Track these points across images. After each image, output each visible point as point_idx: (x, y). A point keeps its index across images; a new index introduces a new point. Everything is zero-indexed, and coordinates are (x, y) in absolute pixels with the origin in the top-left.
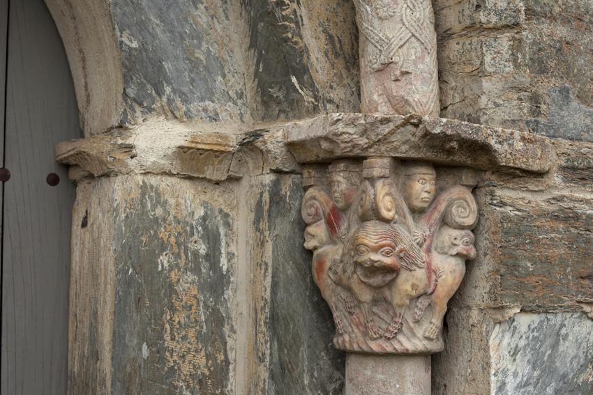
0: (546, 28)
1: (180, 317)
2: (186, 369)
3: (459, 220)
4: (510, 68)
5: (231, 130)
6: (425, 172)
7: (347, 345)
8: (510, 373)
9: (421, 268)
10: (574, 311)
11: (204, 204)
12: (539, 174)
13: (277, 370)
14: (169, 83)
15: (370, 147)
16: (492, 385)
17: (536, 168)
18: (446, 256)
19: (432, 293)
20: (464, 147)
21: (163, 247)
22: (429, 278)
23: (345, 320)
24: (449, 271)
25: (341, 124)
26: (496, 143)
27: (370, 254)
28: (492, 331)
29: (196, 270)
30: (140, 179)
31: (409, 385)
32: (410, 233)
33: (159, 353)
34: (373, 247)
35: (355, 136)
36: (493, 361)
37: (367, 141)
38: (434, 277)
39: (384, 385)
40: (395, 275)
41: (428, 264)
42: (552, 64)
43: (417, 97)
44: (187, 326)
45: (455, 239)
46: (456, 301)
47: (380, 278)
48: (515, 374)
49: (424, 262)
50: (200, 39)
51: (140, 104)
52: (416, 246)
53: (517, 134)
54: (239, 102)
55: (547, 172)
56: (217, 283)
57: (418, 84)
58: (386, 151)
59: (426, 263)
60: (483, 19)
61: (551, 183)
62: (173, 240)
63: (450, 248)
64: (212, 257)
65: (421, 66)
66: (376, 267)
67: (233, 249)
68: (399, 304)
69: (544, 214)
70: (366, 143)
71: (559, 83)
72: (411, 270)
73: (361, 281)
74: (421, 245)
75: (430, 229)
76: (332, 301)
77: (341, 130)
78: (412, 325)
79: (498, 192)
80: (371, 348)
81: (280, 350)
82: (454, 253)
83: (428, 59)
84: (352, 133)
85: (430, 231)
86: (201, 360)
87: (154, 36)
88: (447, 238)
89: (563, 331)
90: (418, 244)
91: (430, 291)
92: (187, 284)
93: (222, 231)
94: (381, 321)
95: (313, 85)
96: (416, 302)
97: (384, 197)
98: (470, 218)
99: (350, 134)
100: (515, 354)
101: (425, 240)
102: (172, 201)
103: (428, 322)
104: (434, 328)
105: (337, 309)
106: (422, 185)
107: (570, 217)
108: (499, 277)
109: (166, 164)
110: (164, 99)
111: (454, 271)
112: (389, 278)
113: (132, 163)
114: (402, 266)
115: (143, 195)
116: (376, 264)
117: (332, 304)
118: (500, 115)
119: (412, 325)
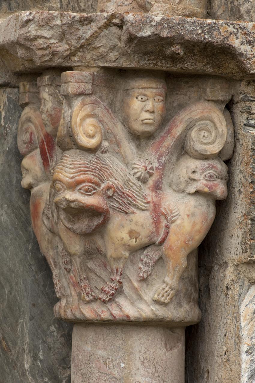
3: (199, 147)
6: (146, 85)
7: (62, 311)
9: (143, 210)
15: (73, 54)
16: (244, 366)
18: (182, 195)
19: (162, 243)
20: (195, 51)
22: (157, 224)
23: (64, 280)
25: (33, 26)
26: (243, 43)
27: (66, 192)
28: (245, 295)
31: (139, 365)
32: (127, 165)
34: (69, 183)
35: (52, 41)
36: (245, 333)
37: (68, 47)
38: (164, 223)
39: (105, 364)
40: (102, 219)
41: (155, 205)
45: (194, 172)
47: (86, 223)
49: (148, 203)
52: (135, 182)
58: (93, 59)
59: (151, 205)
63: (187, 184)
66: (73, 208)
68: (114, 256)
70: (67, 50)
72: (126, 213)
73: (67, 228)
74: (144, 181)
75: (159, 159)
76: (50, 255)
77: (33, 33)
78: (136, 284)
80: (83, 314)
82: (193, 190)
84: (48, 37)
85: (159, 162)
88: (184, 171)
90: (138, 179)
91: (159, 240)
94: (99, 280)
96: (141, 254)
98: (216, 144)
99: (46, 38)
101: (151, 175)
103: (161, 281)
104: (167, 289)
105: (55, 266)
108: (249, 222)
111: (193, 214)
112: (96, 222)
114: (113, 208)
116: (73, 205)
117: (51, 260)
119: (136, 284)
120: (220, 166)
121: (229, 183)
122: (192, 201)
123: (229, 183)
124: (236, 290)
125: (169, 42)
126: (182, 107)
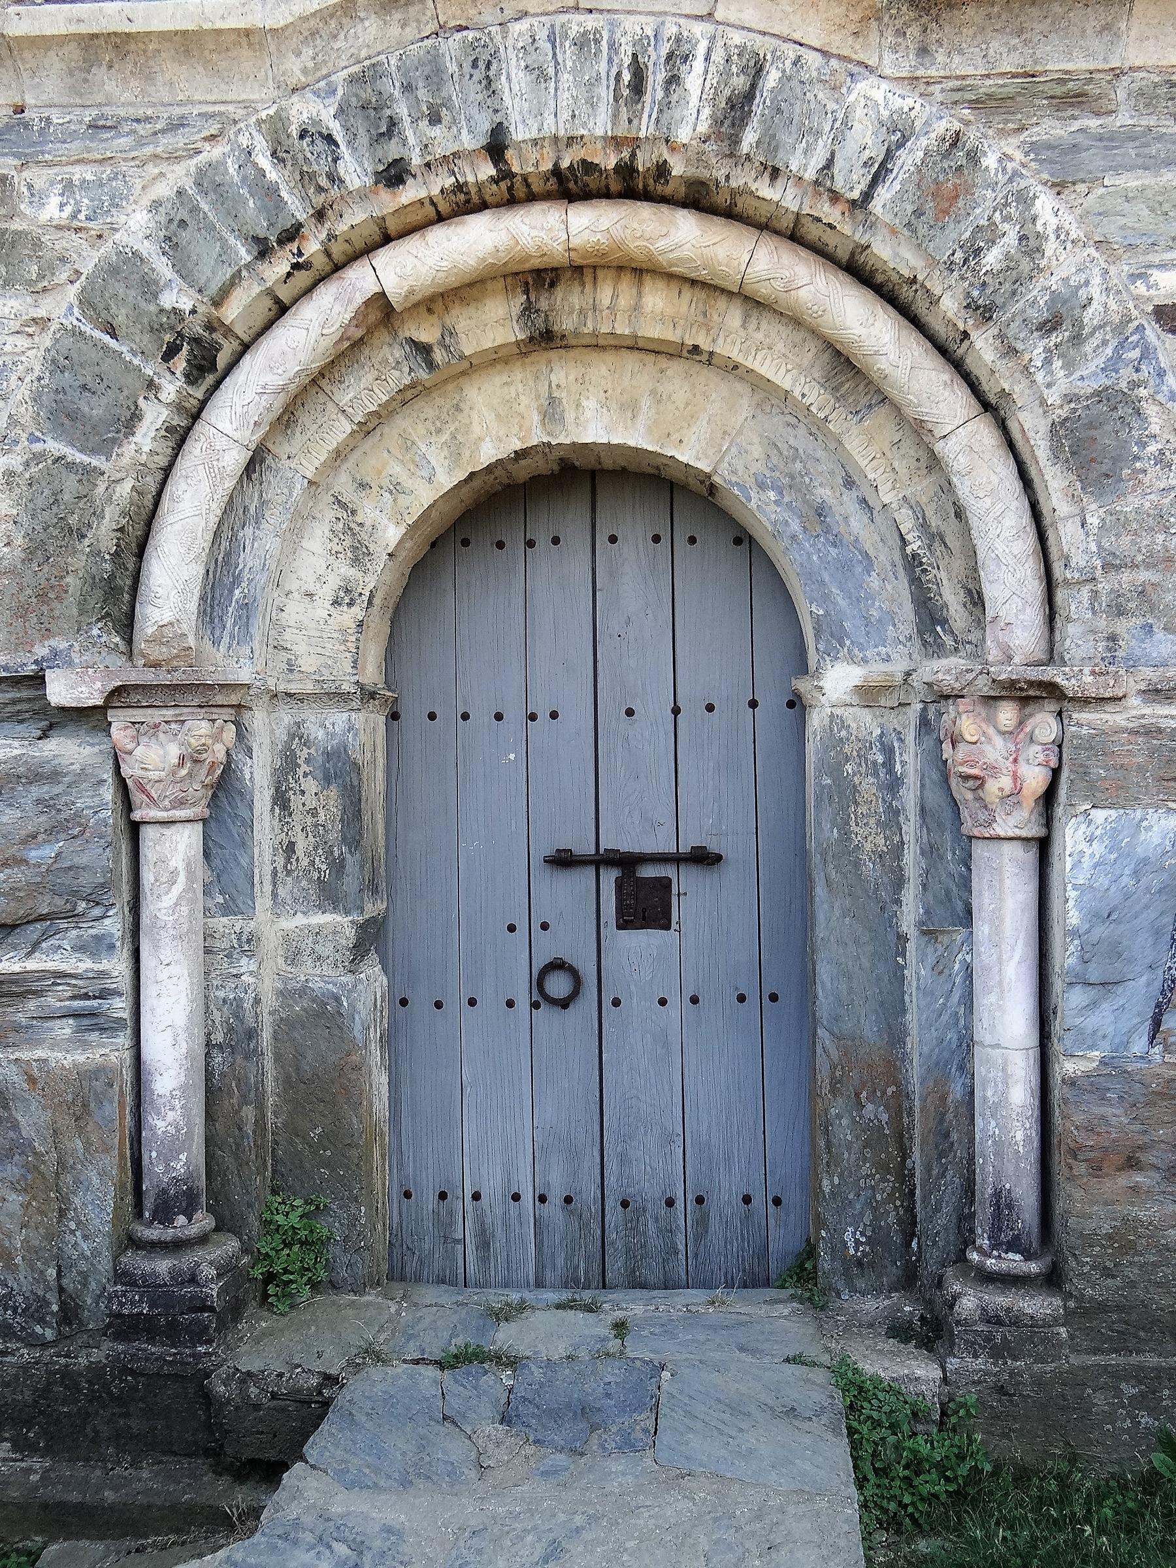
0: (1126, 577)
1: (862, 809)
2: (868, 846)
4: (1089, 615)
5: (898, 667)
8: (1087, 855)
10: (1157, 808)
11: (881, 726)
12: (1120, 699)
13: (927, 848)
14: (848, 638)
17: (1107, 695)
21: (847, 759)
22: (1015, 783)
24: (1035, 779)
29: (876, 774)
30: (829, 710)
33: (846, 835)
42: (1132, 605)
43: (1017, 642)
44: (868, 816)
46: (1049, 797)
48: (1093, 855)
50: (874, 600)
51: (829, 655)
53: (1087, 670)
54: (908, 644)
55: (1125, 696)
56: (894, 784)
57: (1019, 632)
60: (1069, 576)
61: (1129, 705)
62: (855, 753)
64: (889, 764)
65: (1021, 617)
67: (905, 757)
69: (1125, 730)
71: (1140, 621)
79: (1075, 716)
81: (928, 834)
83: (1028, 610)
86: (881, 841)
87: (835, 604)
89: (1145, 823)
92: (868, 786)
93: (896, 745)
95: (952, 632)
97: (968, 727)
100: (1091, 841)
102: (853, 725)
106: (1007, 714)
107: (1151, 731)
109: (848, 699)
110: (846, 649)
113: (823, 699)
115: (831, 722)
118: (1080, 653)
120: (1056, 749)
121: (1060, 759)
122: (1037, 769)
123: (1060, 759)
124: (1063, 820)
125: (1018, 681)
126: (1031, 715)
